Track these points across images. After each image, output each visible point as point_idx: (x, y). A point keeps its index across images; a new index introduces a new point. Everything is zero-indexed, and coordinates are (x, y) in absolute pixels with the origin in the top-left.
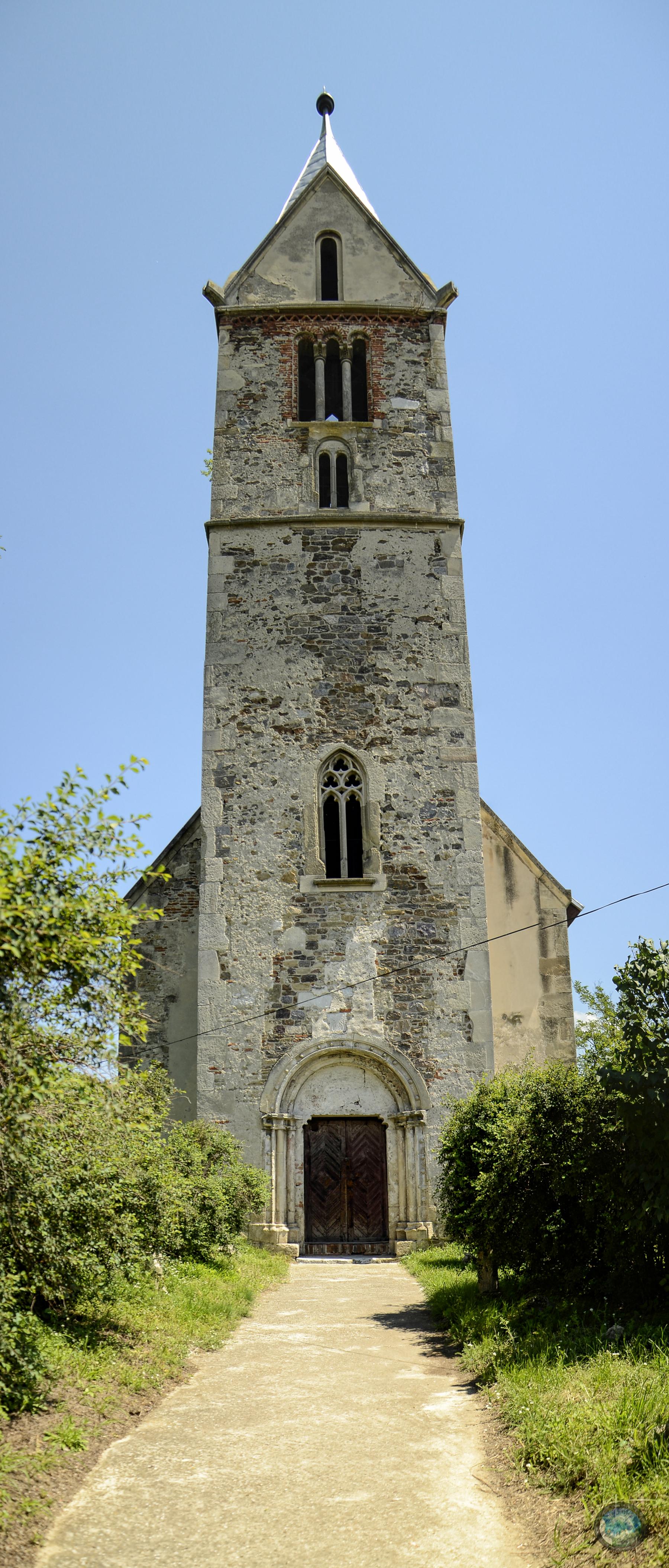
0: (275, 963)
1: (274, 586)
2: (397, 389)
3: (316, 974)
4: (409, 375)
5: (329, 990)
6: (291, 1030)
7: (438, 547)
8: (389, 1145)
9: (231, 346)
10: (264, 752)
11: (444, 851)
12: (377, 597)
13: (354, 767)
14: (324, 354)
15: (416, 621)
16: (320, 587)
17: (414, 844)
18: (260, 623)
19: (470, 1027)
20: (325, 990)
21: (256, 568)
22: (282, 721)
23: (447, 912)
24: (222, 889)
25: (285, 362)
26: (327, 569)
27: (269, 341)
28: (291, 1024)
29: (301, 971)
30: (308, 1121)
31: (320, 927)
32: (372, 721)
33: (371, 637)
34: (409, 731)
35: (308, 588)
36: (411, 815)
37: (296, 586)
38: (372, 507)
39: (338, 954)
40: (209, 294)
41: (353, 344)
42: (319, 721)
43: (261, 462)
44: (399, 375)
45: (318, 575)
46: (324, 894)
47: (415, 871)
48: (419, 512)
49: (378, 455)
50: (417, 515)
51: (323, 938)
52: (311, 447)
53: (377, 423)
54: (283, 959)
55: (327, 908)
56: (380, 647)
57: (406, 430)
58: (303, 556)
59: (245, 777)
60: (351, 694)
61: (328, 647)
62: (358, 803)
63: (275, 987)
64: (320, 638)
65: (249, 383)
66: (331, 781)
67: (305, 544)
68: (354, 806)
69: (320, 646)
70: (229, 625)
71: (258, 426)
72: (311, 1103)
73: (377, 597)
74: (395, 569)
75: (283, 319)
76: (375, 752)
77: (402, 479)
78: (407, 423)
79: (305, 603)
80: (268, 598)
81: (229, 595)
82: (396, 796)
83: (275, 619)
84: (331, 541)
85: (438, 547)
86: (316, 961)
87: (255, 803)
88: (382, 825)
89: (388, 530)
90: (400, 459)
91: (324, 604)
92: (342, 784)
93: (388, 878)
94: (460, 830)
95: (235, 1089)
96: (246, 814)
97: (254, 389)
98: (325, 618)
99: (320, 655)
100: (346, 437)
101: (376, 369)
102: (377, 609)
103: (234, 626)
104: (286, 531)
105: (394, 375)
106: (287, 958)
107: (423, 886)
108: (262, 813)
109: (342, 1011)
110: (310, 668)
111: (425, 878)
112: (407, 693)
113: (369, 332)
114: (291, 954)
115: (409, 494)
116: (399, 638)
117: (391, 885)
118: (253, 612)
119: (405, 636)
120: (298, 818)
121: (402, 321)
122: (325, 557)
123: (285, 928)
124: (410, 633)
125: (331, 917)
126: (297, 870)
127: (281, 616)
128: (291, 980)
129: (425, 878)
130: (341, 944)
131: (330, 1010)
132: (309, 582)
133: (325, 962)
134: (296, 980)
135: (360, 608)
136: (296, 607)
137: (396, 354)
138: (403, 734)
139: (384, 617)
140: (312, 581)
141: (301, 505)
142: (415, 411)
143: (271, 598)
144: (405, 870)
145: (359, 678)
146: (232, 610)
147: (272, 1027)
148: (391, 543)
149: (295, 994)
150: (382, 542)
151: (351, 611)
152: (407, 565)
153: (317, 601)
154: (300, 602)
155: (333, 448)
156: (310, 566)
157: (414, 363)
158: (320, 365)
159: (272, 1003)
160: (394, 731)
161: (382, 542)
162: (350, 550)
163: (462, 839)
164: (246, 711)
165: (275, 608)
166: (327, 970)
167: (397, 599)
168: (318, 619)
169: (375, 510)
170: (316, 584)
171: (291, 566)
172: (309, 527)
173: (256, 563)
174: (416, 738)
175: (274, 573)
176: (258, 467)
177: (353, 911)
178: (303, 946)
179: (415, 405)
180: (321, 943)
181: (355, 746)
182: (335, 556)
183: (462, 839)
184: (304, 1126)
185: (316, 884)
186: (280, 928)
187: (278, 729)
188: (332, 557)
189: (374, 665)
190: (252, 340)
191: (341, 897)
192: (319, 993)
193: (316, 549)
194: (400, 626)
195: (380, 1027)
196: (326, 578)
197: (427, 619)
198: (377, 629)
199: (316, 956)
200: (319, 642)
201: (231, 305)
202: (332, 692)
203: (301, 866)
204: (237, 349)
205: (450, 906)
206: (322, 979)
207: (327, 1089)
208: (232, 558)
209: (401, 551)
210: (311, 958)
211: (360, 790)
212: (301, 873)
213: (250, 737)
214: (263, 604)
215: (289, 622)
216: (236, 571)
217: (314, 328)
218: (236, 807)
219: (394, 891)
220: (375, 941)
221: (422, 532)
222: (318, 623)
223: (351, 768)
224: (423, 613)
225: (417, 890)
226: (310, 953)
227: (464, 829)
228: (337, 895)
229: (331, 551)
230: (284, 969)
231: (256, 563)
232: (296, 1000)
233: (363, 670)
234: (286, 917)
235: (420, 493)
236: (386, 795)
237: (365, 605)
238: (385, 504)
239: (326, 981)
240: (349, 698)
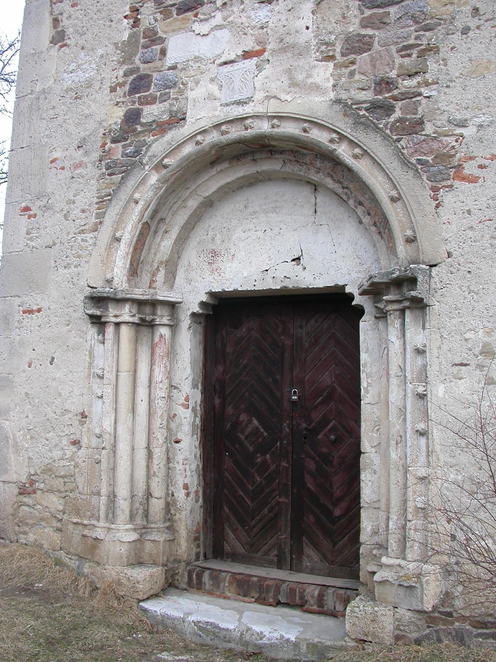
5: (225, 19)
6: (152, 112)
8: (364, 357)
20: (218, 18)
28: (152, 101)
30: (203, 304)
63: (131, 36)
72: (206, 266)
95: (55, 244)
109: (247, 55)
128: (159, 16)
131: (222, 60)
147: (120, 113)
149: (162, 40)
159: (125, 67)
184: (194, 315)
192: (204, 28)
195: (323, 74)
207: (238, 234)
232: (163, 52)
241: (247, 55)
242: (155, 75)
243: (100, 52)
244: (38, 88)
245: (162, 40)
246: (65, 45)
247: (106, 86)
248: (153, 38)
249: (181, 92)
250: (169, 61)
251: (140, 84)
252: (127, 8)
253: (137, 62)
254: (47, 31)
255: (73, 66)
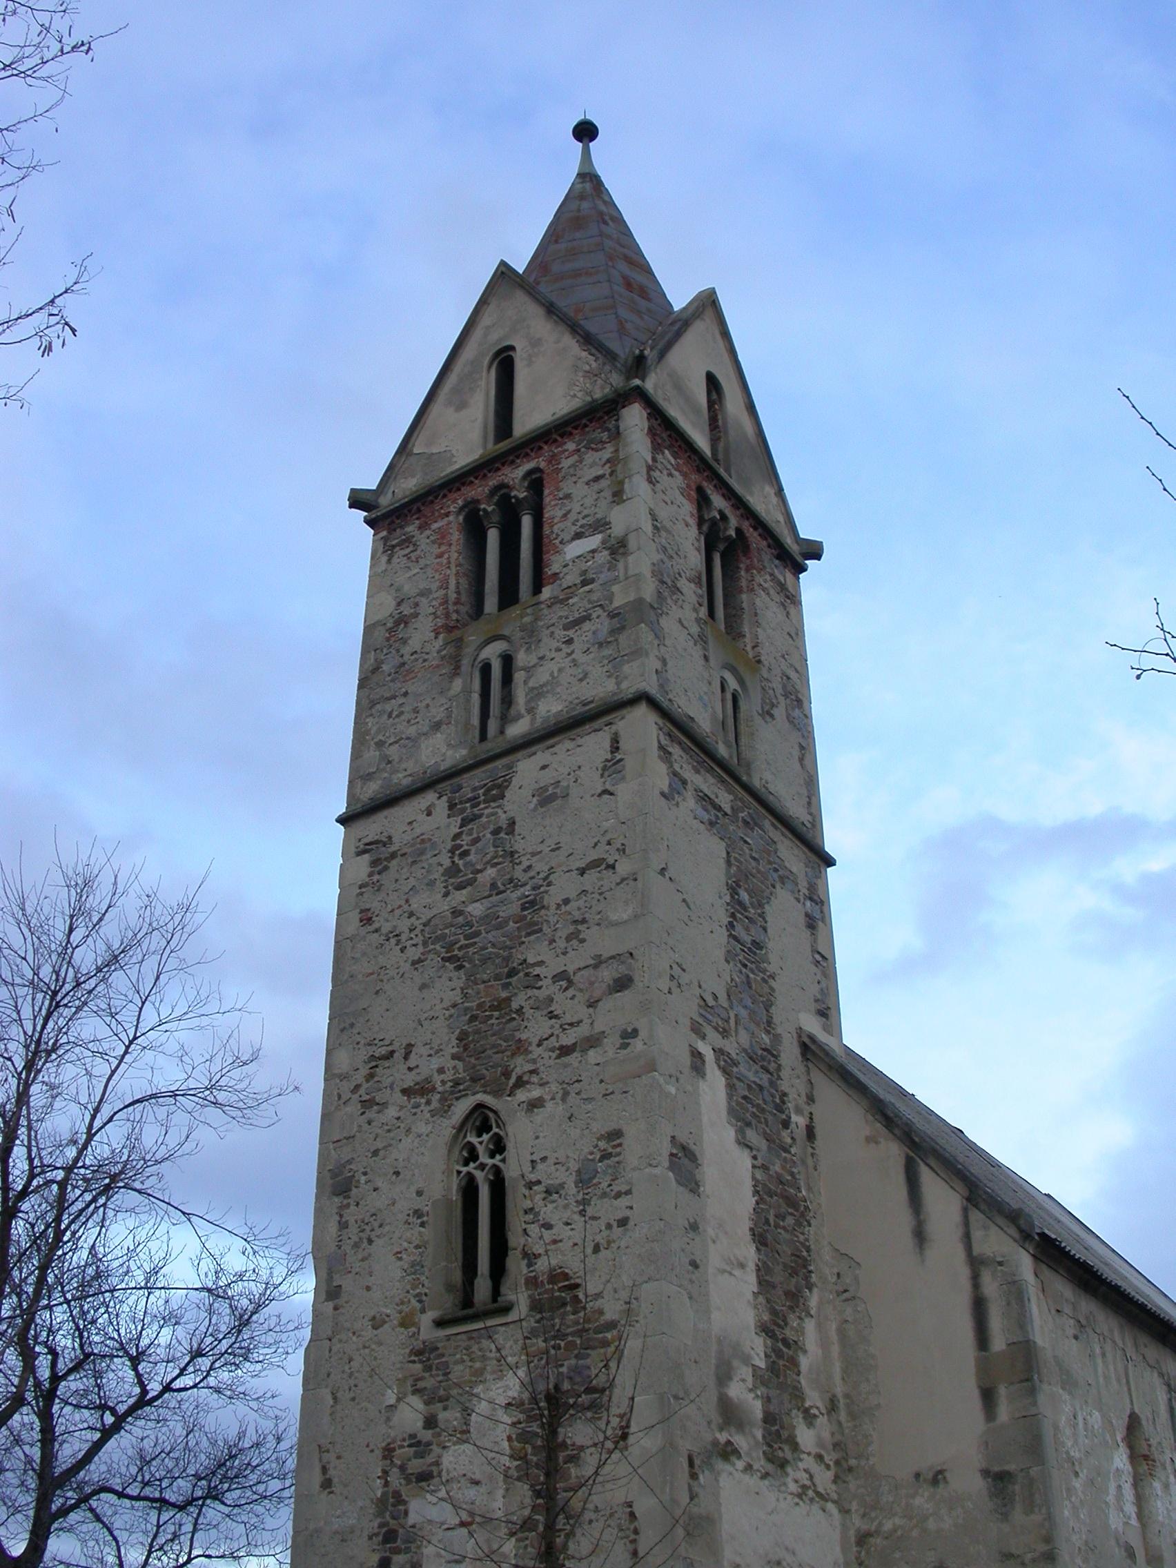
0: (385, 1458)
1: (412, 882)
2: (574, 528)
3: (434, 1468)
4: (589, 501)
7: (615, 748)
9: (384, 559)
10: (389, 1131)
11: (605, 1233)
12: (533, 854)
13: (498, 1126)
14: (495, 518)
15: (582, 872)
16: (465, 865)
17: (565, 1232)
18: (393, 941)
19: (636, 1532)
21: (394, 862)
22: (410, 1080)
23: (609, 1335)
24: (330, 1351)
25: (440, 556)
26: (475, 835)
27: (428, 532)
28: (397, 1551)
29: (416, 1466)
31: (442, 1392)
32: (518, 1048)
33: (525, 916)
34: (565, 1051)
35: (453, 871)
36: (562, 1186)
37: (437, 874)
38: (533, 720)
39: (463, 1432)
40: (358, 500)
41: (528, 489)
42: (454, 1067)
43: (406, 708)
44: (576, 507)
45: (466, 847)
46: (448, 1338)
47: (566, 1276)
48: (592, 702)
49: (545, 640)
50: (592, 705)
51: (445, 1409)
52: (466, 662)
53: (547, 592)
54: (394, 1450)
55: (451, 1359)
56: (533, 929)
57: (585, 583)
58: (448, 826)
59: (365, 1174)
60: (496, 1014)
61: (471, 950)
62: (503, 1179)
63: (384, 1494)
64: (463, 942)
65: (399, 604)
66: (472, 1156)
67: (452, 806)
68: (498, 1185)
69: (460, 954)
70: (358, 955)
71: (406, 657)
73: (533, 854)
74: (559, 801)
75: (445, 496)
76: (522, 1095)
77: (574, 660)
78: (584, 572)
79: (446, 895)
80: (403, 903)
81: (362, 911)
82: (544, 1159)
83: (411, 931)
84: (481, 792)
85: (615, 747)
86: (434, 1447)
87: (373, 1211)
88: (526, 1212)
89: (552, 746)
90: (571, 633)
91: (469, 888)
92: (484, 1158)
93: (530, 1296)
94: (628, 1192)
96: (363, 1231)
97: (406, 610)
98: (470, 909)
99: (460, 967)
100: (506, 632)
101: (552, 511)
102: (532, 873)
103: (364, 954)
104: (430, 797)
105: (570, 511)
106: (402, 1447)
107: (576, 1299)
108: (381, 1226)
109: (463, 1524)
110: (448, 988)
111: (577, 1286)
112: (566, 989)
113: (543, 465)
114: (404, 1440)
115: (581, 680)
116: (558, 906)
117: (536, 1306)
118: (384, 931)
119: (566, 901)
120: (422, 1225)
121: (586, 426)
122: (475, 818)
123: (399, 1400)
124: (573, 895)
125: (458, 1372)
126: (418, 1306)
127: (417, 923)
128: (403, 1482)
129: (577, 1286)
130: (467, 1412)
132: (453, 862)
133: (444, 1447)
134: (408, 1479)
135: (511, 880)
136: (434, 904)
137: (574, 479)
138: (558, 1057)
139: (541, 882)
140: (456, 859)
141: (450, 753)
142: (593, 551)
143: (407, 901)
144: (557, 1276)
145: (506, 986)
146: (363, 931)
148: (555, 765)
150: (544, 767)
151: (502, 888)
152: (574, 791)
153: (459, 887)
154: (440, 896)
155: (492, 652)
156: (457, 836)
157: (597, 479)
158: (493, 536)
159: (379, 1520)
160: (546, 1055)
161: (544, 767)
162: (503, 797)
163: (631, 1208)
164: (370, 1076)
165: (411, 914)
166: (448, 1460)
167: (558, 848)
168: (461, 913)
169: (539, 721)
170: (461, 862)
171: (434, 845)
172: (455, 781)
173: (393, 856)
174: (573, 1059)
175: (414, 862)
176: (403, 717)
177: (484, 1358)
178: (420, 1424)
179: (594, 541)
180: (442, 1416)
181: (497, 1093)
182: (486, 812)
183: (631, 1208)
185: (440, 1323)
186: (392, 1401)
187: (406, 1092)
188: (480, 816)
189: (525, 960)
190: (408, 541)
191: (471, 1338)
193: (464, 810)
194: (564, 886)
195: (509, 1547)
196: (473, 849)
197: (595, 864)
198: (532, 903)
199: (434, 1440)
200: (460, 949)
201: (385, 501)
202: (474, 1018)
203: (424, 1298)
204: (389, 561)
205: (612, 1325)
206: (440, 1475)
208: (366, 856)
209: (566, 771)
210: (429, 1444)
211: (503, 1160)
212: (423, 1311)
213: (371, 1114)
214: (398, 912)
215: (427, 929)
216: (371, 875)
217: (478, 490)
218: (352, 1221)
219: (539, 1316)
220: (509, 1404)
221: (595, 731)
222: (461, 919)
223: (495, 1130)
224: (594, 855)
225: (569, 1308)
226: (427, 1435)
227: (634, 1190)
228: (464, 1337)
229: (482, 806)
230: (395, 1466)
231: (393, 856)
232: (406, 1513)
233: (512, 973)
234: (401, 1382)
235: (597, 672)
236: (532, 1161)
237: (518, 873)
238: (551, 708)
239: (445, 1477)
240: (493, 1021)
241: (463, 1524)
242: (401, 1531)
243: (360, 1504)
244: (312, 1526)
245: (405, 1503)
246: (332, 1492)
247: (366, 1533)
248: (399, 1499)
249: (419, 1547)
250: (411, 1521)
251: (390, 1536)
252: (379, 1470)
253: (388, 1518)
254: (317, 1478)
255: (339, 1512)
